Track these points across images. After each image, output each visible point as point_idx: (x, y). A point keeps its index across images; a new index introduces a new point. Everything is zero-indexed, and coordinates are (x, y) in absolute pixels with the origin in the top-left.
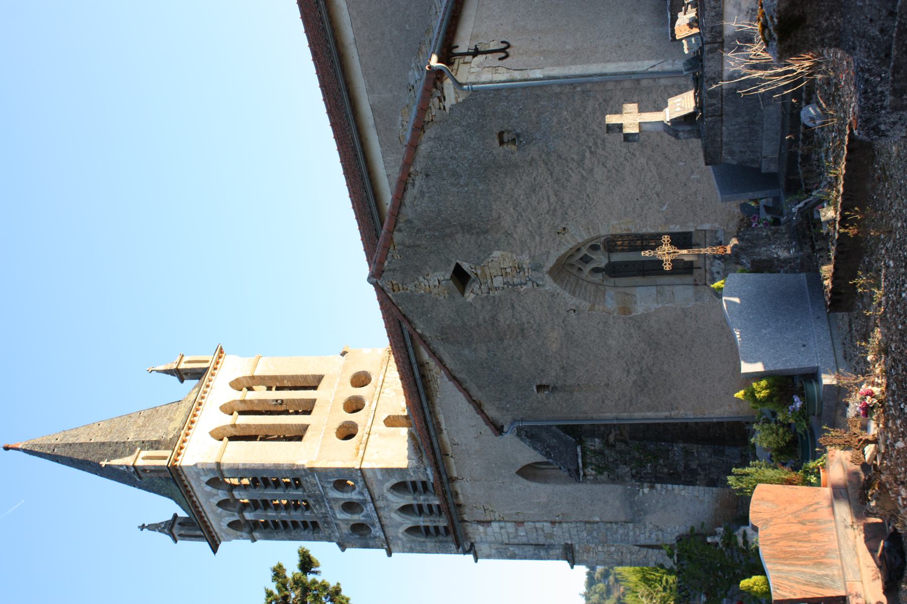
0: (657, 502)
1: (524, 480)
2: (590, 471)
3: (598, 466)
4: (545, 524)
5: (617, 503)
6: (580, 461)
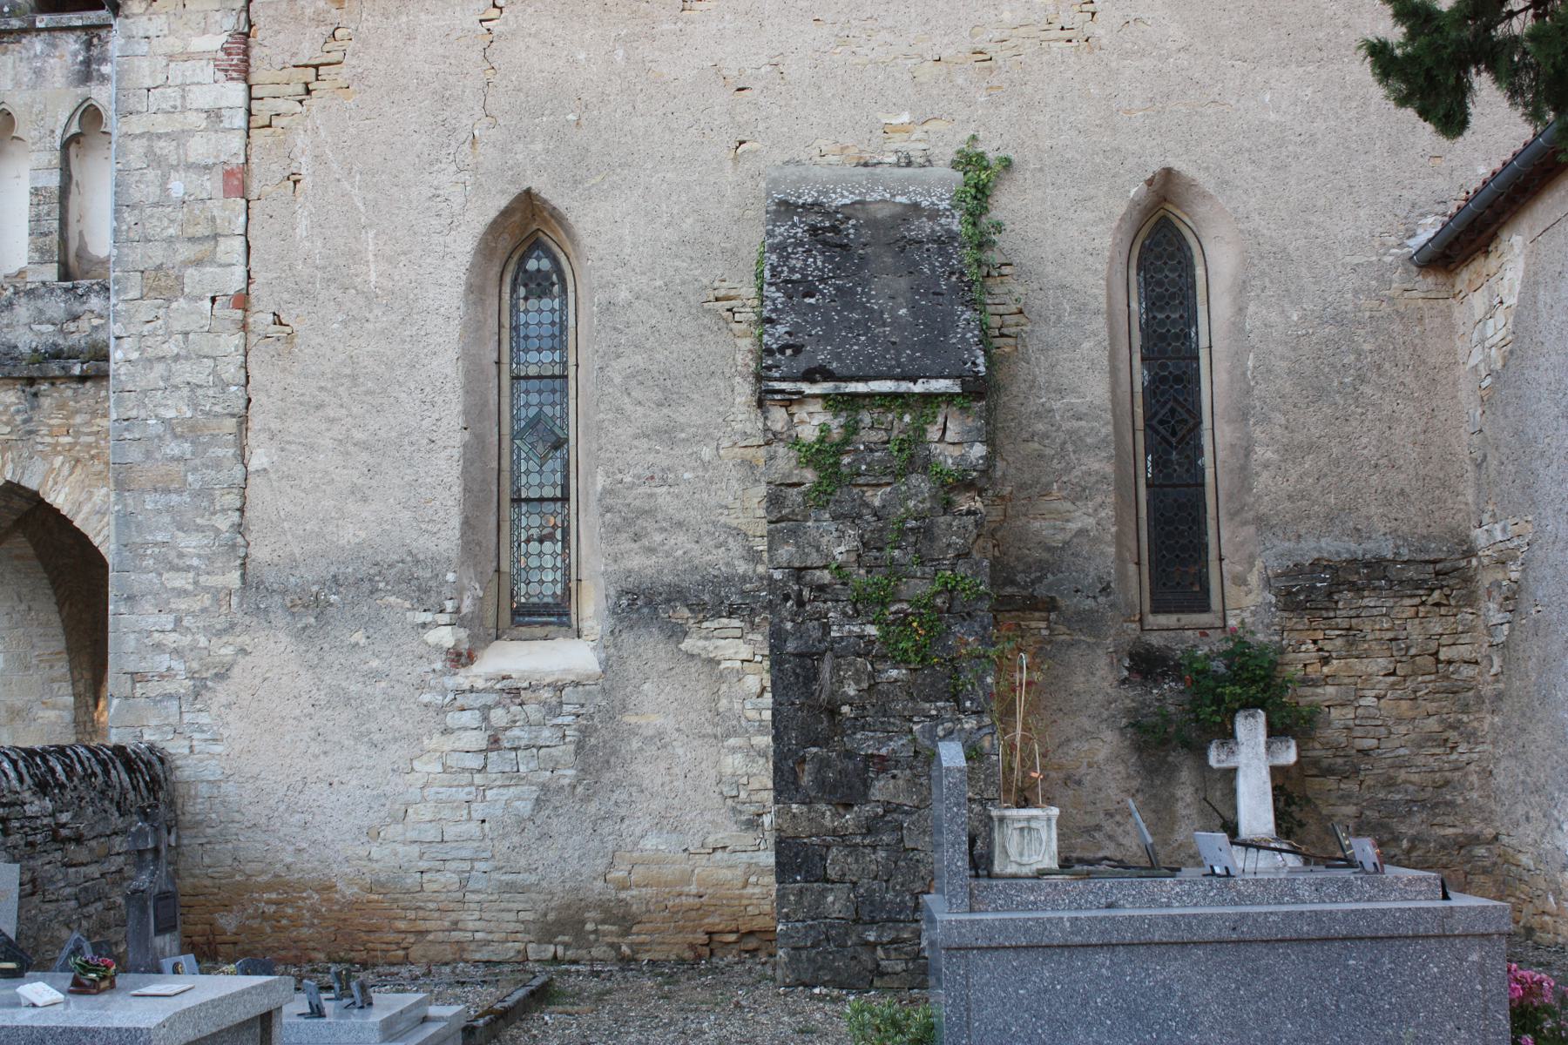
0: (375, 676)
1: (493, 214)
2: (812, 422)
3: (839, 449)
4: (240, 271)
5: (349, 535)
6: (861, 387)
